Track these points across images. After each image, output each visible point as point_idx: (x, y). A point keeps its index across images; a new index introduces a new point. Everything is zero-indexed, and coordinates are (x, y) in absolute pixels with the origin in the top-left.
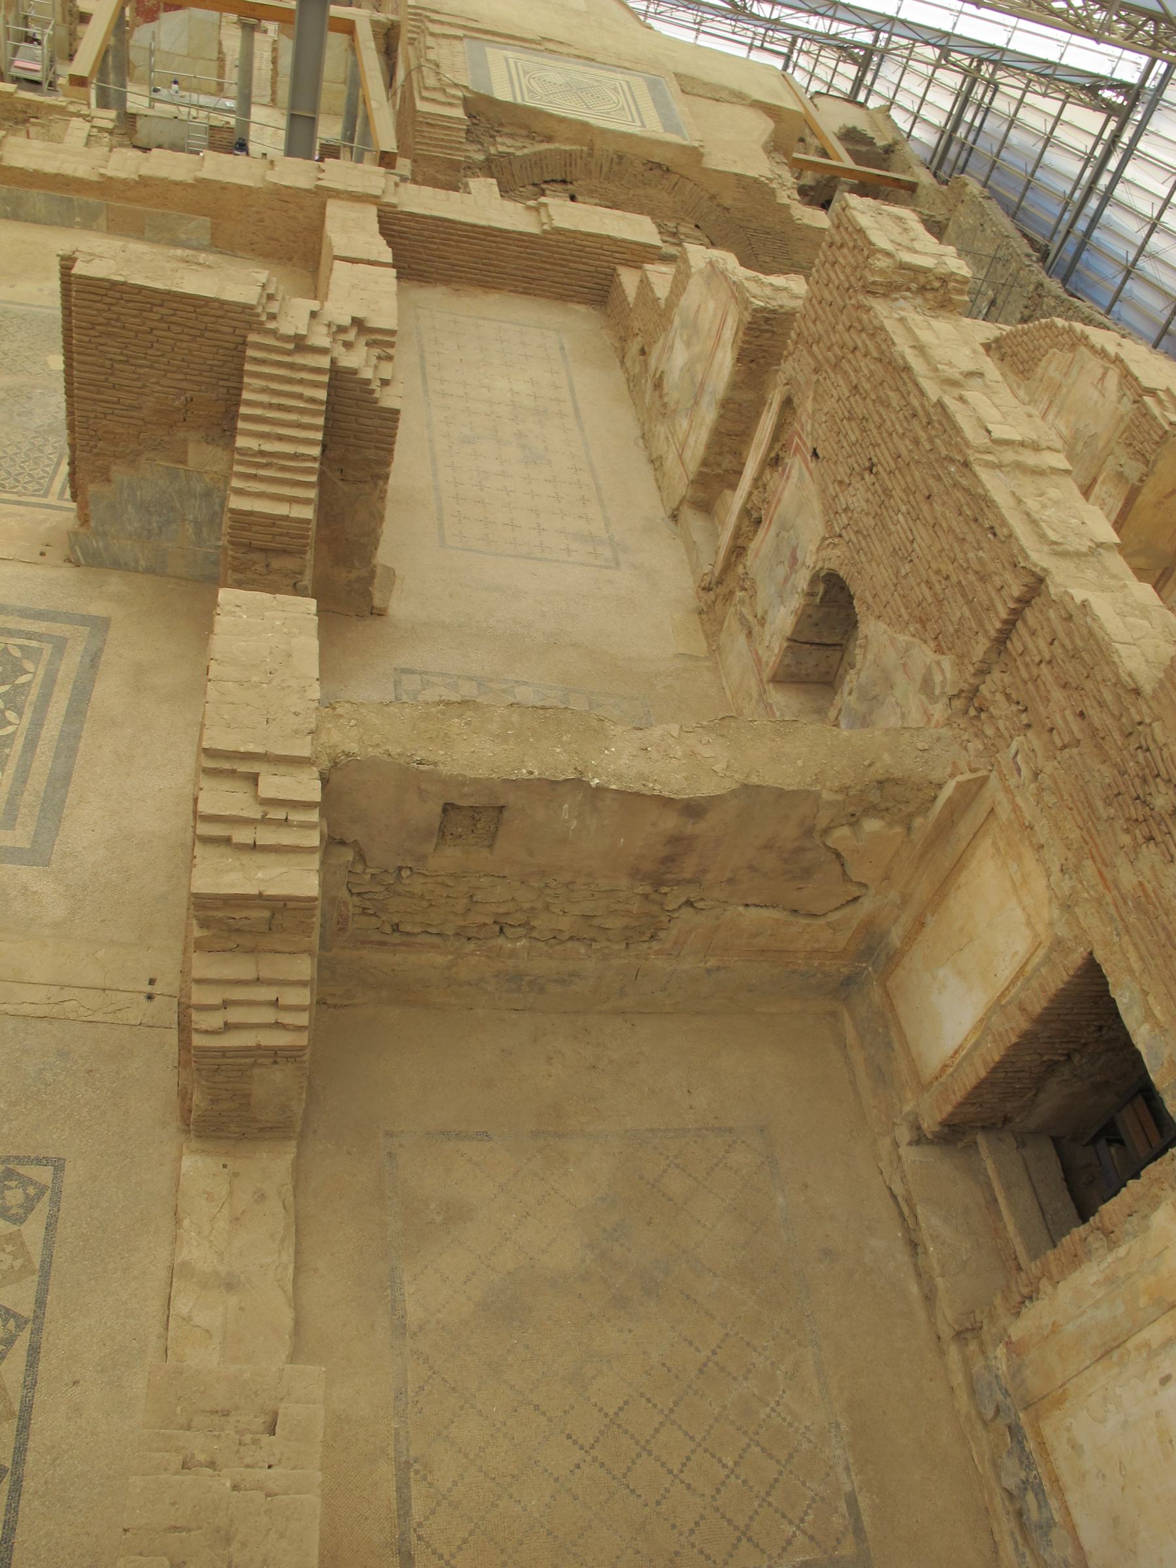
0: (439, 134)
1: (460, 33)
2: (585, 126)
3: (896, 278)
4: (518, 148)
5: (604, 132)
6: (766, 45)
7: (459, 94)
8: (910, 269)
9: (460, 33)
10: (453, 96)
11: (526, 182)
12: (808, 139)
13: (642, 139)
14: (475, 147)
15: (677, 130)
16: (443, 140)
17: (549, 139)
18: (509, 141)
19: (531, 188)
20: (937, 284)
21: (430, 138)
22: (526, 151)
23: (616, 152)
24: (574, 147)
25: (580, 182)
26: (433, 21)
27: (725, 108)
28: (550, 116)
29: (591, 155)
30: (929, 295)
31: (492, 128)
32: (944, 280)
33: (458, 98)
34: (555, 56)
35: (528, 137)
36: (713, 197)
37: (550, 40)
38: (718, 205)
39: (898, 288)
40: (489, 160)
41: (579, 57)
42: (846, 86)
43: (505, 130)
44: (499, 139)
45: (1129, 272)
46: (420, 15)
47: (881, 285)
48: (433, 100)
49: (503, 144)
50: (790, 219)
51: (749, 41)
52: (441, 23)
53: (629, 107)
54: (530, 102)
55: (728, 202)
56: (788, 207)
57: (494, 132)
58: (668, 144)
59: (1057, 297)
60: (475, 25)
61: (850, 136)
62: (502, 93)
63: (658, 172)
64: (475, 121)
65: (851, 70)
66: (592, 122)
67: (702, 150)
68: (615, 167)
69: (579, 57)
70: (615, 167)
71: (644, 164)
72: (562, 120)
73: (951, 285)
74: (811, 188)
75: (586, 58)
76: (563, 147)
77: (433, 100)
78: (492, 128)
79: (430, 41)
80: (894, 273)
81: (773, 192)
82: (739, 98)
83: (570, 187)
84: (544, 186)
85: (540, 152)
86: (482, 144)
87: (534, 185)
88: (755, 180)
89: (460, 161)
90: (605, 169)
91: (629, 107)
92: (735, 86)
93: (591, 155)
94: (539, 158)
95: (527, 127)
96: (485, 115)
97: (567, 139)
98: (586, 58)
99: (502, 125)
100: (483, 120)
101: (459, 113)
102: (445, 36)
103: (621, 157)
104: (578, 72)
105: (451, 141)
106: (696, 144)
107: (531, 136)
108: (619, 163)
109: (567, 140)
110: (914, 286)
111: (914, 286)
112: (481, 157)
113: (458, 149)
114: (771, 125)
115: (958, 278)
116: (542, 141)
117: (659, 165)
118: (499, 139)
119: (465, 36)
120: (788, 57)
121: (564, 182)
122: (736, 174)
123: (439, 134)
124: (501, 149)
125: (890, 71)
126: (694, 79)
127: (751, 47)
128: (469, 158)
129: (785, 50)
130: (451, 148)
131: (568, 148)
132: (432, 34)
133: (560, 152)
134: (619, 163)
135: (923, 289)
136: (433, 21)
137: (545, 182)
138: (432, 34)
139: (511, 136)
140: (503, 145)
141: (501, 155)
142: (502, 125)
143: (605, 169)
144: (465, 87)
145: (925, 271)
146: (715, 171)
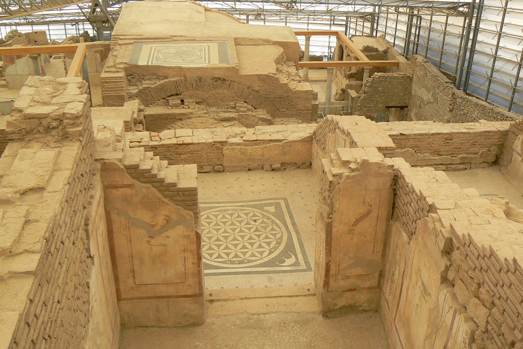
0: (111, 85)
1: (132, 41)
2: (180, 68)
3: (23, 126)
4: (152, 84)
5: (189, 69)
6: (335, 23)
7: (122, 66)
8: (33, 118)
9: (132, 41)
10: (119, 68)
11: (160, 98)
12: (350, 55)
13: (207, 68)
14: (133, 88)
15: (227, 62)
16: (114, 88)
17: (166, 77)
18: (147, 82)
19: (162, 100)
20: (54, 124)
21: (108, 88)
22: (156, 85)
23: (197, 77)
24: (177, 79)
25: (184, 93)
26: (121, 39)
27: (260, 48)
28: (164, 67)
29: (186, 81)
30: (54, 132)
31: (140, 78)
32: (60, 119)
33: (122, 68)
34: (177, 42)
35: (157, 78)
36: (249, 87)
37: (175, 36)
38: (253, 90)
39: (28, 133)
40: (140, 91)
41: (188, 40)
42: (368, 31)
43: (146, 78)
44: (143, 82)
45: (490, 80)
46: (116, 38)
47: (14, 133)
48: (110, 72)
49: (145, 84)
50: (289, 90)
51: (307, 22)
52: (125, 39)
53: (205, 57)
54: (155, 63)
55: (257, 88)
56: (286, 84)
57: (141, 78)
58: (220, 68)
59: (461, 98)
60: (140, 37)
61: (367, 50)
62: (142, 62)
63: (219, 82)
64: (132, 76)
65: (368, 25)
66: (184, 66)
67: (237, 68)
68: (199, 83)
69: (188, 40)
70: (199, 83)
71: (212, 79)
72: (169, 68)
73: (65, 121)
74: (355, 74)
75: (191, 40)
76: (172, 80)
77: (110, 72)
78: (140, 78)
79: (117, 47)
80: (22, 123)
81: (277, 79)
82: (267, 42)
83: (180, 96)
84: (168, 98)
85: (162, 84)
86: (136, 85)
87: (164, 99)
88: (267, 75)
89: (123, 95)
90: (194, 85)
91: (205, 57)
92: (265, 38)
93: (186, 81)
94: (163, 86)
95: (155, 74)
96: (134, 73)
97: (174, 76)
98: (191, 40)
99: (144, 76)
100: (136, 75)
101: (122, 74)
102: (125, 44)
103: (200, 79)
104: (184, 46)
105: (117, 88)
106: (234, 66)
107: (158, 78)
108: (200, 81)
109: (174, 76)
110: (41, 129)
111: (41, 129)
112: (136, 91)
113: (121, 90)
114: (282, 50)
115: (68, 116)
116: (164, 79)
117: (219, 79)
118: (143, 82)
119: (135, 42)
120: (346, 26)
121: (177, 94)
122: (257, 75)
123: (111, 85)
124: (144, 86)
125: (382, 22)
126: (245, 38)
127: (330, 25)
128: (130, 93)
129: (344, 23)
130: (118, 90)
131: (175, 79)
132: (119, 45)
133: (171, 82)
134: (200, 81)
135: (48, 129)
136: (121, 39)
137: (168, 96)
138: (119, 45)
139: (149, 79)
140: (146, 84)
141: (145, 89)
142: (144, 76)
143: (194, 85)
144: (126, 63)
145: (45, 116)
146: (246, 75)
